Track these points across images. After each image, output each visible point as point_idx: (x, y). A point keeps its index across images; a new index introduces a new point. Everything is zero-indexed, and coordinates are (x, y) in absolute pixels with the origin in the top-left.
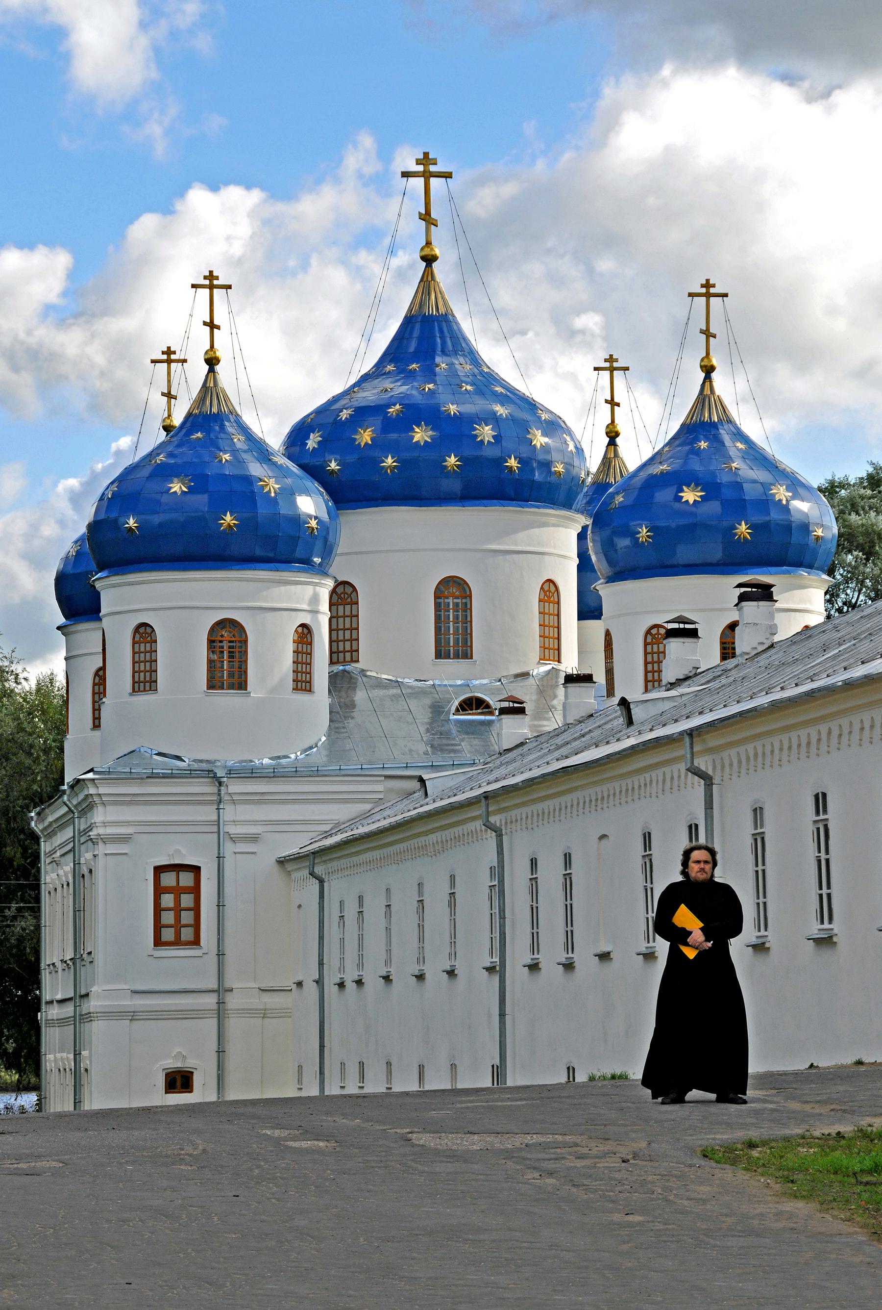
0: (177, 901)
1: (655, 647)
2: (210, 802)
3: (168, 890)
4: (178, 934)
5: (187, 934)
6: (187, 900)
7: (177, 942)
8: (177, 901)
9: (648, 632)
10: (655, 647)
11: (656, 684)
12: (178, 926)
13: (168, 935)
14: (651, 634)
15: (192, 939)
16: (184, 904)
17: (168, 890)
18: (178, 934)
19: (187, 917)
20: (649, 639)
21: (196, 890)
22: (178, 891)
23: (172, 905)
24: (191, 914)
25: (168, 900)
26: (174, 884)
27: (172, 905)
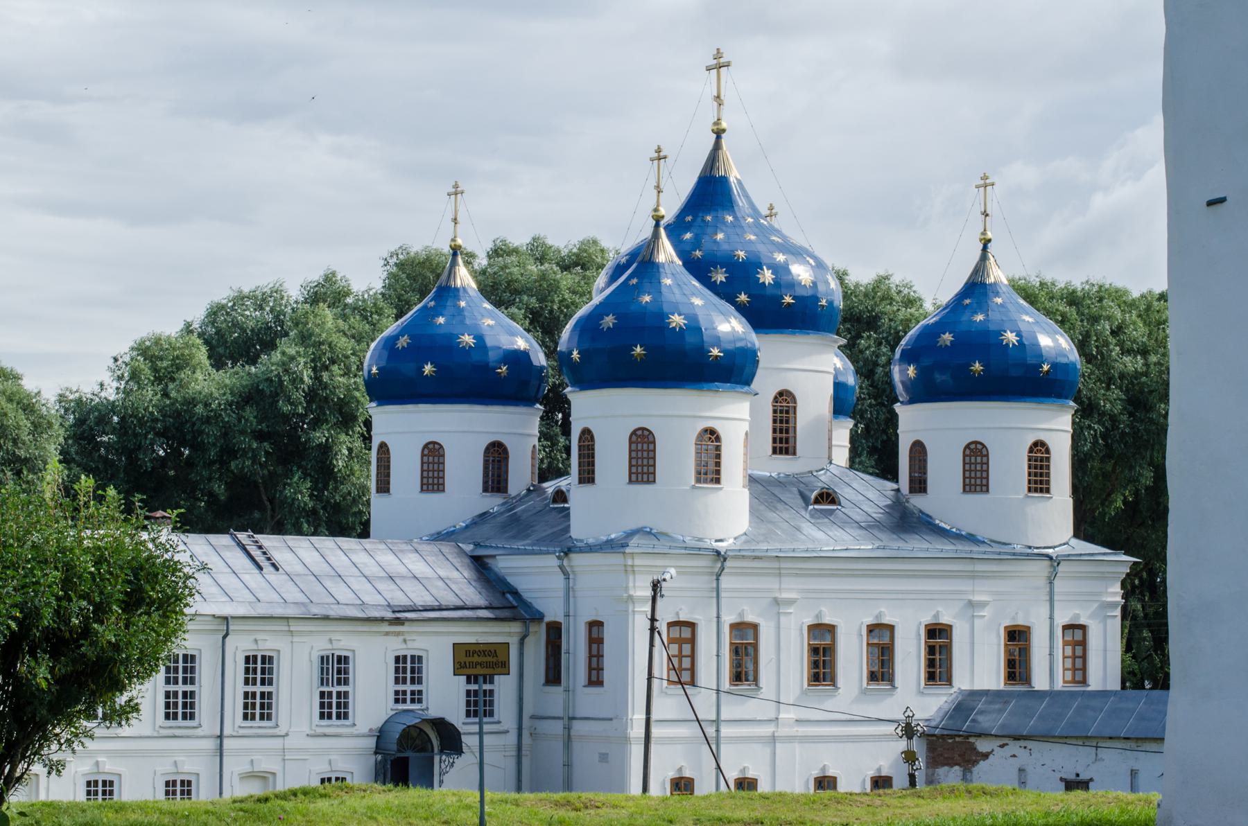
1: (973, 459)
2: (711, 574)
5: (686, 677)
6: (687, 649)
8: (680, 650)
9: (967, 446)
10: (973, 459)
11: (973, 488)
14: (969, 449)
16: (684, 653)
20: (968, 452)
21: (692, 641)
23: (676, 653)
24: (689, 660)
26: (678, 636)
27: (676, 653)
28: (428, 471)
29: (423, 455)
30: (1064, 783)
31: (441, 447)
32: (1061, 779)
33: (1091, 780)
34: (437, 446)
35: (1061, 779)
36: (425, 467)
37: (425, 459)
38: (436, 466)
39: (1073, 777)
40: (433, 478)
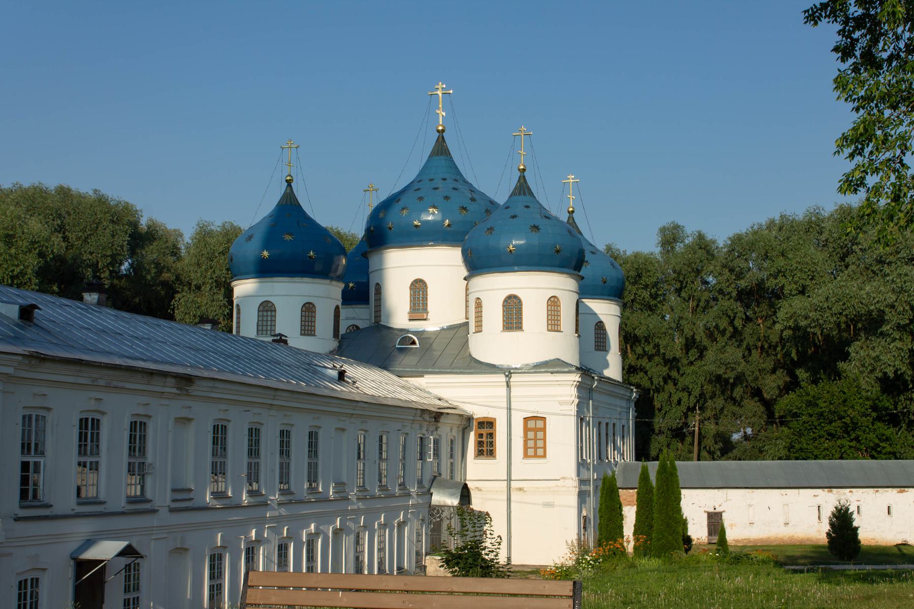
0: (536, 435)
3: (531, 430)
4: (536, 452)
5: (540, 452)
6: (540, 435)
7: (536, 456)
8: (536, 435)
12: (536, 448)
13: (531, 452)
15: (542, 454)
17: (531, 430)
18: (536, 452)
19: (540, 444)
22: (536, 430)
23: (533, 437)
25: (531, 435)
26: (534, 427)
27: (533, 437)
28: (305, 321)
29: (302, 311)
30: (706, 514)
31: (314, 306)
32: (705, 512)
33: (724, 511)
34: (311, 306)
35: (705, 512)
36: (303, 319)
37: (304, 313)
38: (307, 320)
39: (712, 510)
40: (308, 326)
